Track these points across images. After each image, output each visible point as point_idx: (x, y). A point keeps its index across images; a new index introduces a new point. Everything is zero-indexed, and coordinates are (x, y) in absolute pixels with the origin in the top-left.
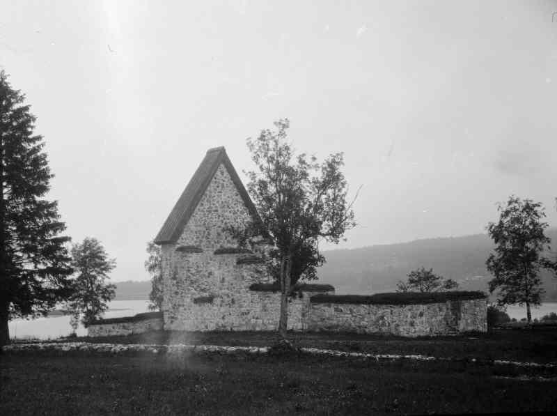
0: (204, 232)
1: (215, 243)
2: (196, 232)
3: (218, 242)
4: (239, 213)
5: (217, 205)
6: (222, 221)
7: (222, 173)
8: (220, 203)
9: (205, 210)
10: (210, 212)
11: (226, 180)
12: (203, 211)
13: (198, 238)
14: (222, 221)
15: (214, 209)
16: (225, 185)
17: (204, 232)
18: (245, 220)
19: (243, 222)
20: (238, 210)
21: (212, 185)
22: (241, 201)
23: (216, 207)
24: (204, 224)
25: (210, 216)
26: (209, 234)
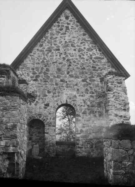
0: (42, 68)
1: (54, 77)
2: (33, 69)
3: (58, 77)
4: (85, 50)
5: (60, 45)
6: (64, 59)
7: (67, 18)
8: (63, 42)
9: (45, 50)
10: (50, 51)
11: (72, 23)
12: (41, 51)
13: (34, 73)
14: (64, 59)
15: (55, 48)
16: (70, 27)
17: (42, 68)
18: (93, 56)
19: (91, 58)
20: (85, 48)
21: (53, 28)
22: (90, 39)
23: (59, 47)
24: (43, 62)
25: (50, 54)
26: (48, 70)
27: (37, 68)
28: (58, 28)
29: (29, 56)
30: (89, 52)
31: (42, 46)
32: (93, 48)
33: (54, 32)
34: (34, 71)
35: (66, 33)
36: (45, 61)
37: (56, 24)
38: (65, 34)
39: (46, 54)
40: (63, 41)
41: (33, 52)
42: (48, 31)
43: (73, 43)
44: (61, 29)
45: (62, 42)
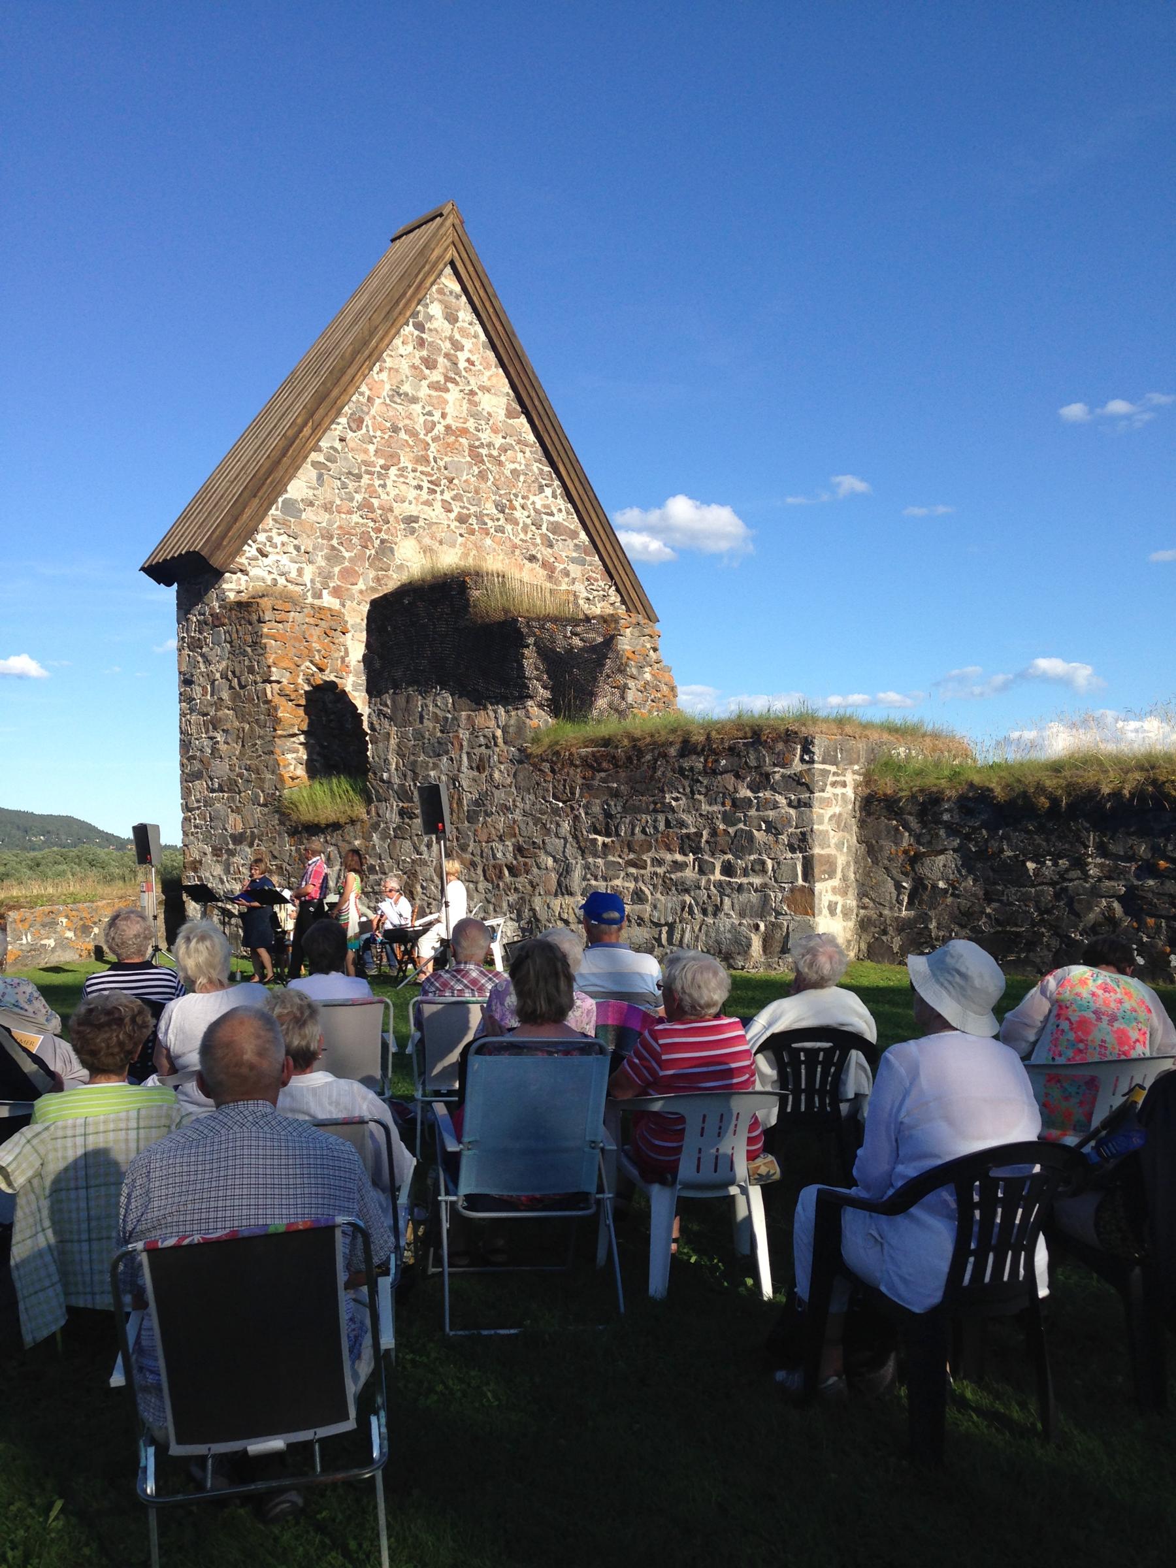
9: (372, 448)
13: (334, 556)
25: (393, 471)
27: (346, 533)
28: (417, 354)
29: (307, 466)
30: (532, 498)
31: (359, 428)
32: (544, 482)
33: (404, 366)
34: (333, 548)
35: (450, 385)
36: (376, 502)
37: (409, 329)
38: (448, 390)
39: (378, 469)
40: (439, 423)
41: (323, 444)
42: (379, 358)
43: (477, 443)
44: (430, 364)
45: (434, 424)
